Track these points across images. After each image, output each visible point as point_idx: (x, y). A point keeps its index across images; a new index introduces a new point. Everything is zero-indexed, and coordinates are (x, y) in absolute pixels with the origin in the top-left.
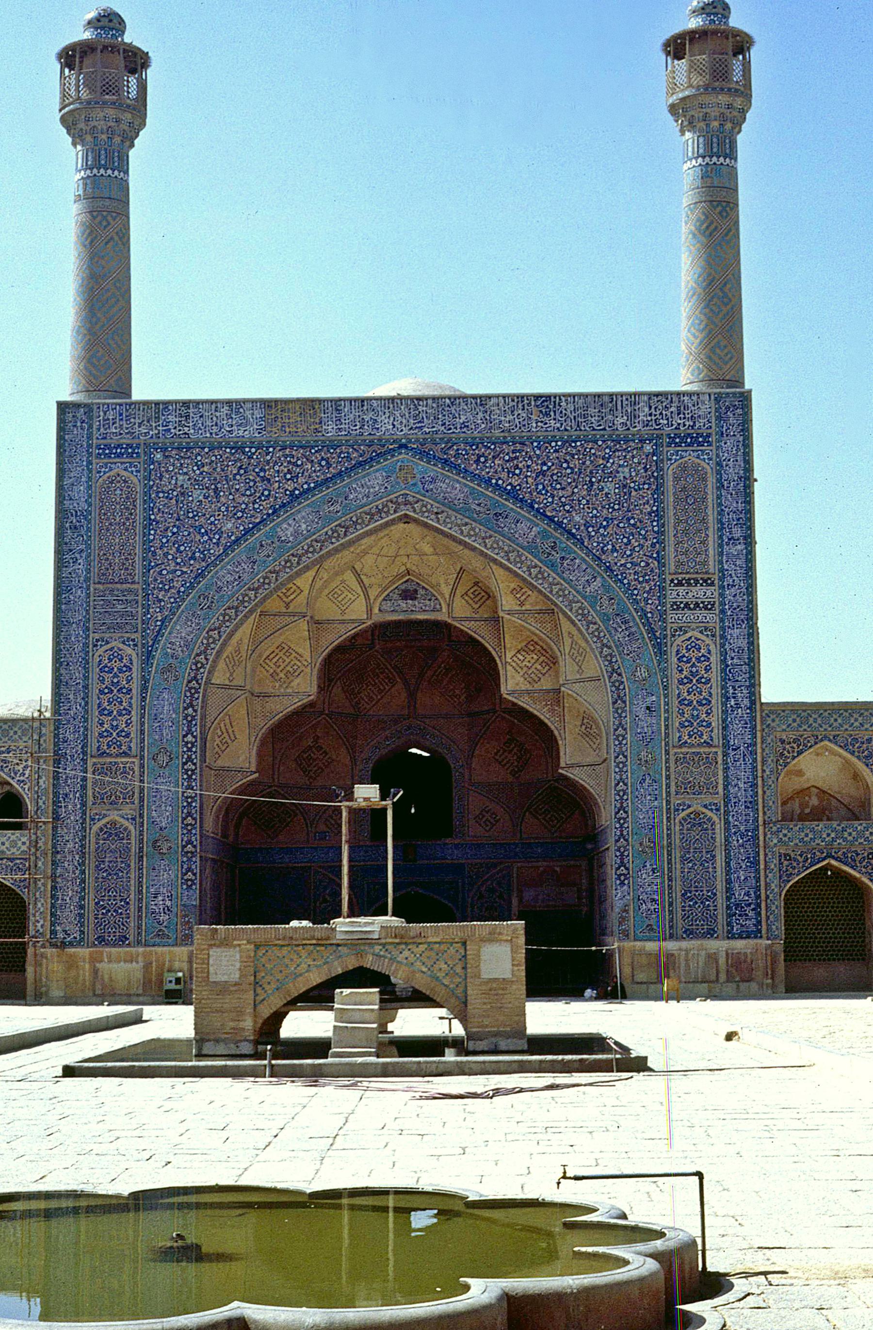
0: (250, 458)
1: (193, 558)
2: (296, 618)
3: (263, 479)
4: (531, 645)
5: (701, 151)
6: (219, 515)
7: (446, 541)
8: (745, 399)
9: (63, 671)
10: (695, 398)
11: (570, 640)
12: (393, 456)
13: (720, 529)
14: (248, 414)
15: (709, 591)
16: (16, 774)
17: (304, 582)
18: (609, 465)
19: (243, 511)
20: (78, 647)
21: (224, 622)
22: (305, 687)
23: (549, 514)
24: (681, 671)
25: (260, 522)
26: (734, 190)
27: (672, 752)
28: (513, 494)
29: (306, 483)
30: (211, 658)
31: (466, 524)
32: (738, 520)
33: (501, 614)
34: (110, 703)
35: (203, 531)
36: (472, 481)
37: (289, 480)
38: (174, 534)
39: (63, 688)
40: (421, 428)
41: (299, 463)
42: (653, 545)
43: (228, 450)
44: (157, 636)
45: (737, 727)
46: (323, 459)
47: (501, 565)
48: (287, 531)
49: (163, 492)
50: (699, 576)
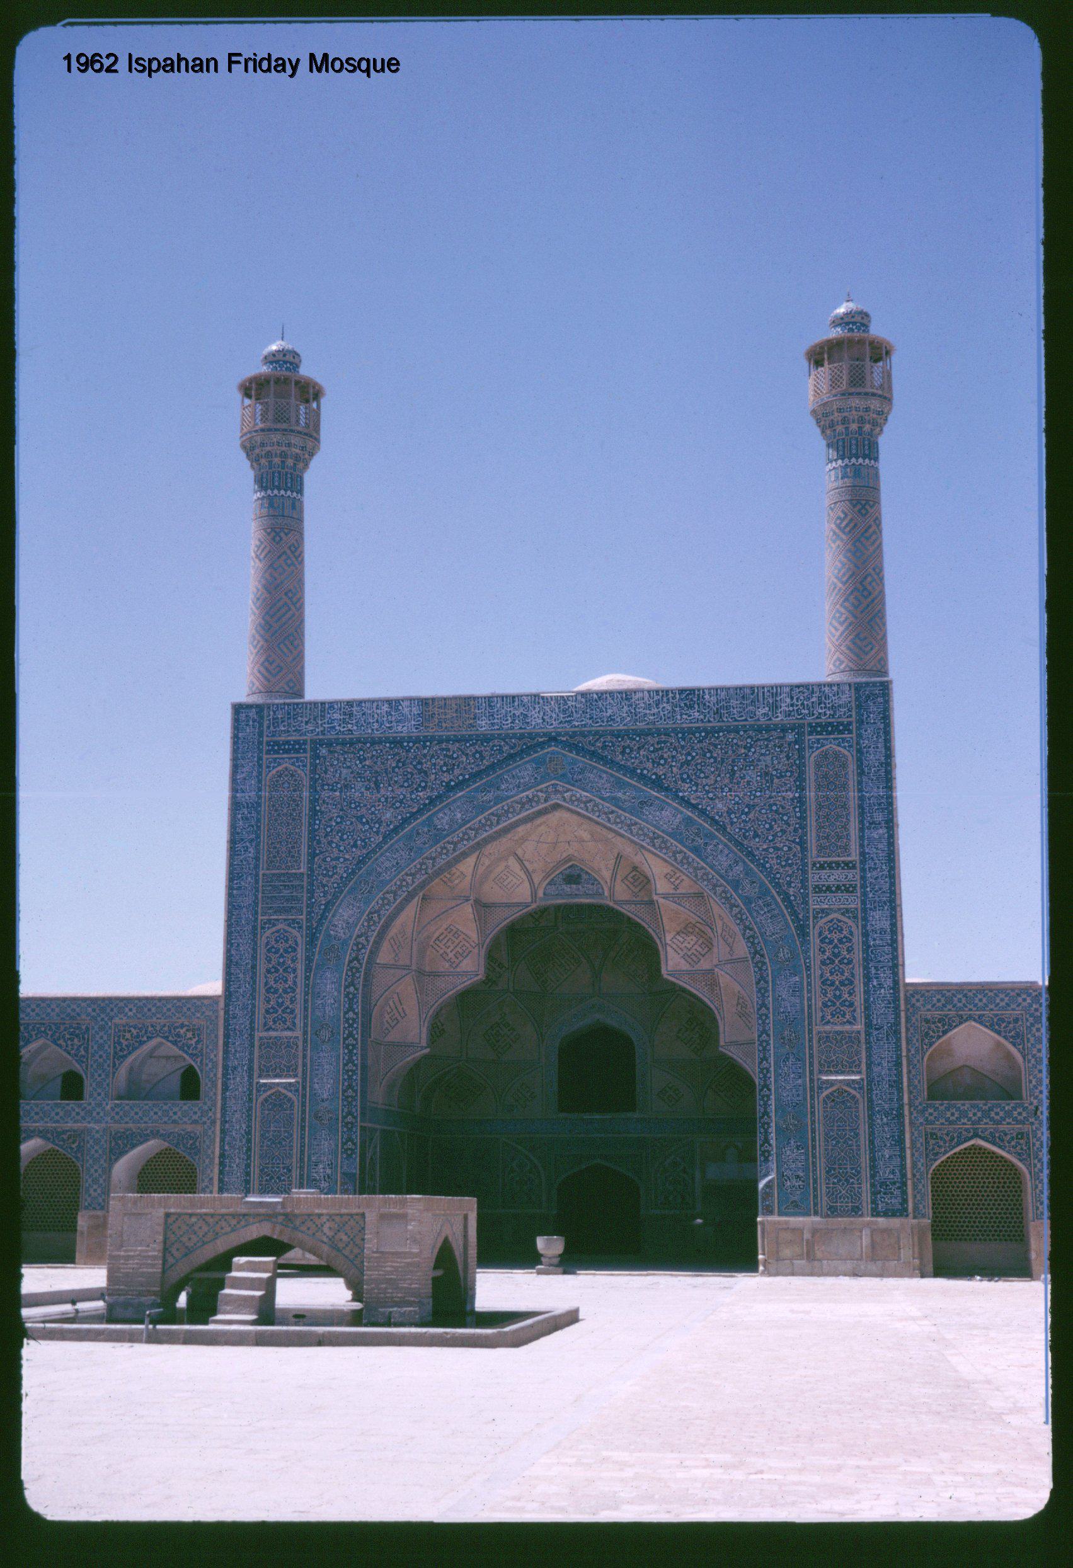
0: (408, 751)
1: (355, 845)
3: (420, 771)
4: (686, 929)
7: (598, 829)
8: (885, 689)
9: (233, 952)
10: (835, 688)
12: (542, 749)
15: (850, 874)
17: (467, 866)
18: (750, 754)
19: (401, 802)
21: (383, 905)
22: (471, 968)
23: (693, 802)
24: (824, 952)
26: (876, 489)
28: (657, 783)
30: (372, 940)
31: (612, 812)
32: (880, 804)
33: (655, 898)
34: (276, 981)
36: (617, 771)
38: (337, 823)
40: (569, 722)
42: (795, 830)
45: (880, 1007)
46: (477, 752)
47: (649, 851)
48: (443, 821)
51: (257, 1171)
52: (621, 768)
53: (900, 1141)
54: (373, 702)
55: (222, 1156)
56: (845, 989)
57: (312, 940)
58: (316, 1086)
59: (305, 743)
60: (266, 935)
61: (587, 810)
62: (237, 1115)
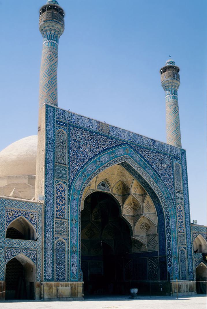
0: (94, 136)
1: (81, 161)
9: (47, 189)
13: (183, 181)
14: (93, 123)
16: (32, 221)
20: (51, 182)
25: (97, 154)
28: (148, 162)
31: (139, 167)
35: (83, 153)
37: (103, 145)
38: (76, 152)
39: (47, 194)
41: (105, 141)
45: (188, 229)
49: (73, 139)
50: (180, 191)
51: (55, 267)
52: (141, 156)
53: (192, 262)
54: (85, 117)
55: (45, 261)
56: (182, 223)
58: (72, 238)
59: (67, 124)
60: (57, 184)
61: (133, 166)
62: (49, 247)
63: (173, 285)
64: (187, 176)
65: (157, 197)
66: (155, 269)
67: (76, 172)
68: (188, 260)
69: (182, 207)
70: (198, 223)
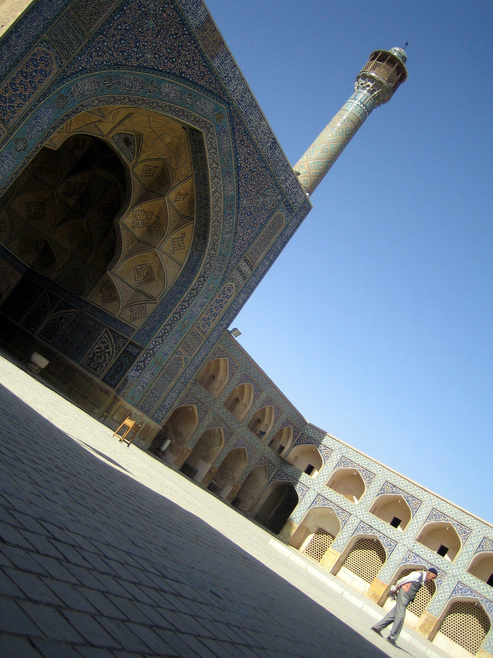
0: (183, 34)
2: (99, 114)
5: (362, 101)
6: (150, 45)
11: (181, 236)
12: (223, 103)
13: (269, 251)
14: (200, 12)
25: (160, 71)
27: (194, 328)
28: (238, 168)
29: (190, 75)
31: (217, 164)
35: (138, 44)
37: (186, 65)
38: (126, 29)
43: (179, 19)
44: (74, 74)
46: (203, 72)
48: (165, 89)
50: (252, 264)
52: (235, 147)
57: (62, 79)
61: (209, 150)
63: (119, 403)
64: (282, 249)
65: (205, 238)
66: (106, 354)
67: (96, 63)
68: (176, 384)
69: (234, 291)
70: (238, 339)
